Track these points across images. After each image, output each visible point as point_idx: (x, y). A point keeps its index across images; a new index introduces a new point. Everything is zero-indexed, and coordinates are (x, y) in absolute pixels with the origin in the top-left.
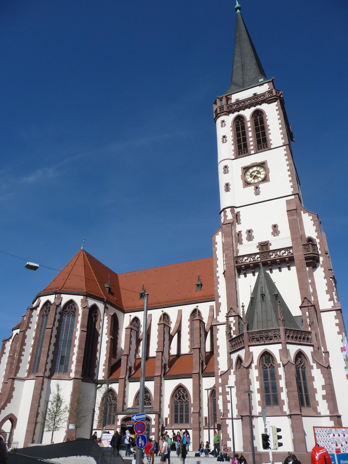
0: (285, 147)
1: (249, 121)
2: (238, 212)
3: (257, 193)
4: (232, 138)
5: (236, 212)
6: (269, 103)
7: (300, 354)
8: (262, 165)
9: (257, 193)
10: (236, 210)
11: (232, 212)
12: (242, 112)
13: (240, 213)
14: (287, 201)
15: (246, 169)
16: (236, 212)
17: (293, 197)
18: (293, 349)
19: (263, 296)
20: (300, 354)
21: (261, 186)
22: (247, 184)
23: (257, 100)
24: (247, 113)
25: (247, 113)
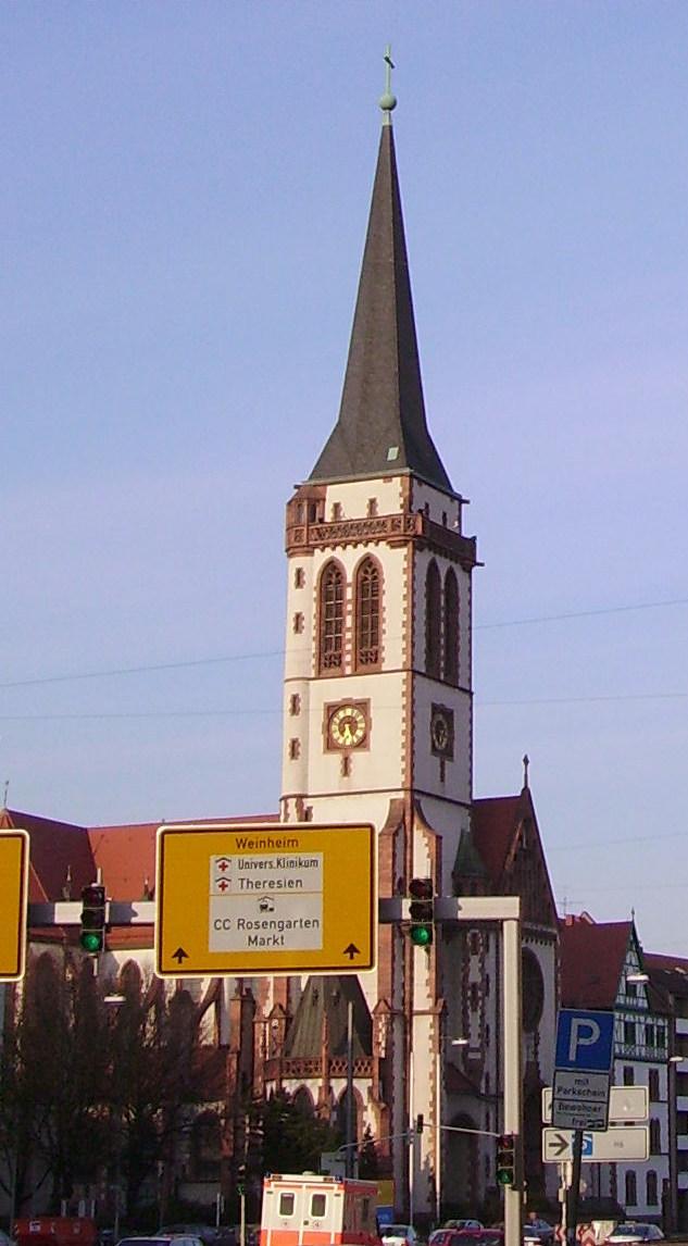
0: (404, 674)
1: (349, 585)
2: (310, 808)
3: (346, 771)
4: (314, 622)
5: (305, 808)
6: (392, 547)
7: (350, 1092)
8: (363, 706)
9: (346, 771)
10: (308, 803)
11: (299, 806)
12: (338, 554)
13: (313, 811)
14: (392, 801)
15: (332, 710)
16: (305, 808)
17: (401, 795)
18: (338, 1086)
19: (316, 992)
20: (350, 1092)
21: (357, 757)
22: (330, 746)
23: (370, 528)
24: (349, 558)
25: (349, 558)
